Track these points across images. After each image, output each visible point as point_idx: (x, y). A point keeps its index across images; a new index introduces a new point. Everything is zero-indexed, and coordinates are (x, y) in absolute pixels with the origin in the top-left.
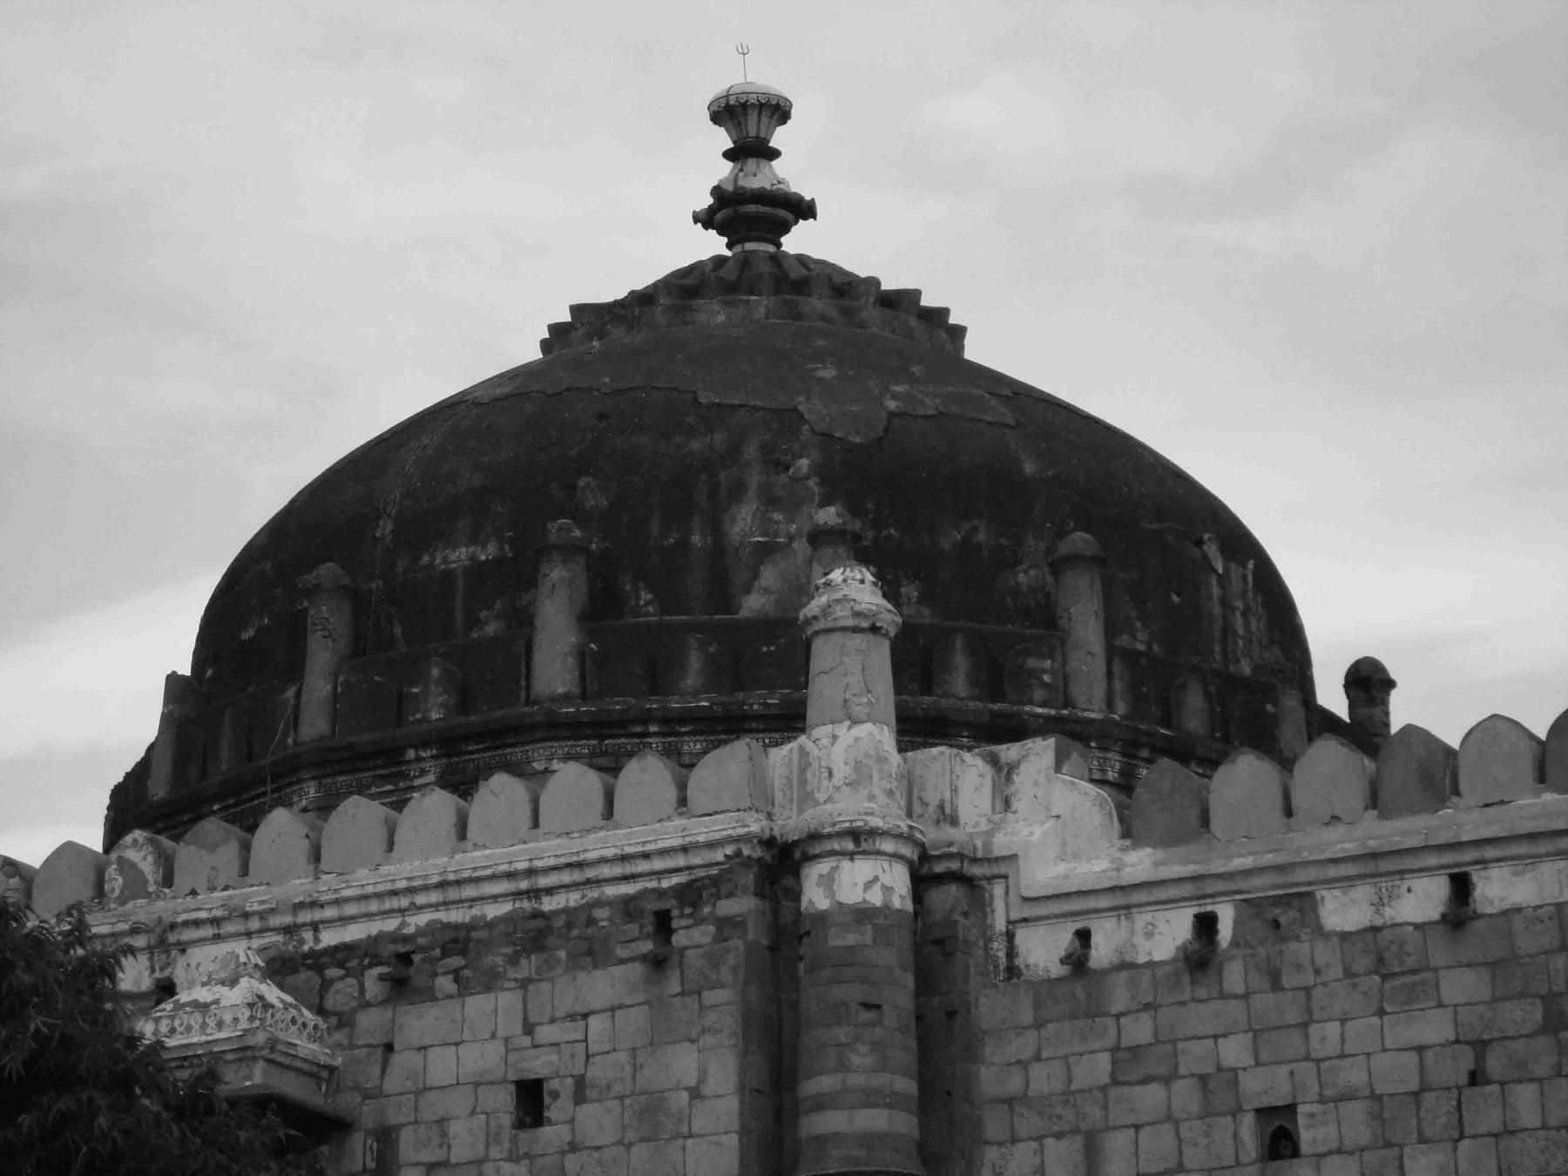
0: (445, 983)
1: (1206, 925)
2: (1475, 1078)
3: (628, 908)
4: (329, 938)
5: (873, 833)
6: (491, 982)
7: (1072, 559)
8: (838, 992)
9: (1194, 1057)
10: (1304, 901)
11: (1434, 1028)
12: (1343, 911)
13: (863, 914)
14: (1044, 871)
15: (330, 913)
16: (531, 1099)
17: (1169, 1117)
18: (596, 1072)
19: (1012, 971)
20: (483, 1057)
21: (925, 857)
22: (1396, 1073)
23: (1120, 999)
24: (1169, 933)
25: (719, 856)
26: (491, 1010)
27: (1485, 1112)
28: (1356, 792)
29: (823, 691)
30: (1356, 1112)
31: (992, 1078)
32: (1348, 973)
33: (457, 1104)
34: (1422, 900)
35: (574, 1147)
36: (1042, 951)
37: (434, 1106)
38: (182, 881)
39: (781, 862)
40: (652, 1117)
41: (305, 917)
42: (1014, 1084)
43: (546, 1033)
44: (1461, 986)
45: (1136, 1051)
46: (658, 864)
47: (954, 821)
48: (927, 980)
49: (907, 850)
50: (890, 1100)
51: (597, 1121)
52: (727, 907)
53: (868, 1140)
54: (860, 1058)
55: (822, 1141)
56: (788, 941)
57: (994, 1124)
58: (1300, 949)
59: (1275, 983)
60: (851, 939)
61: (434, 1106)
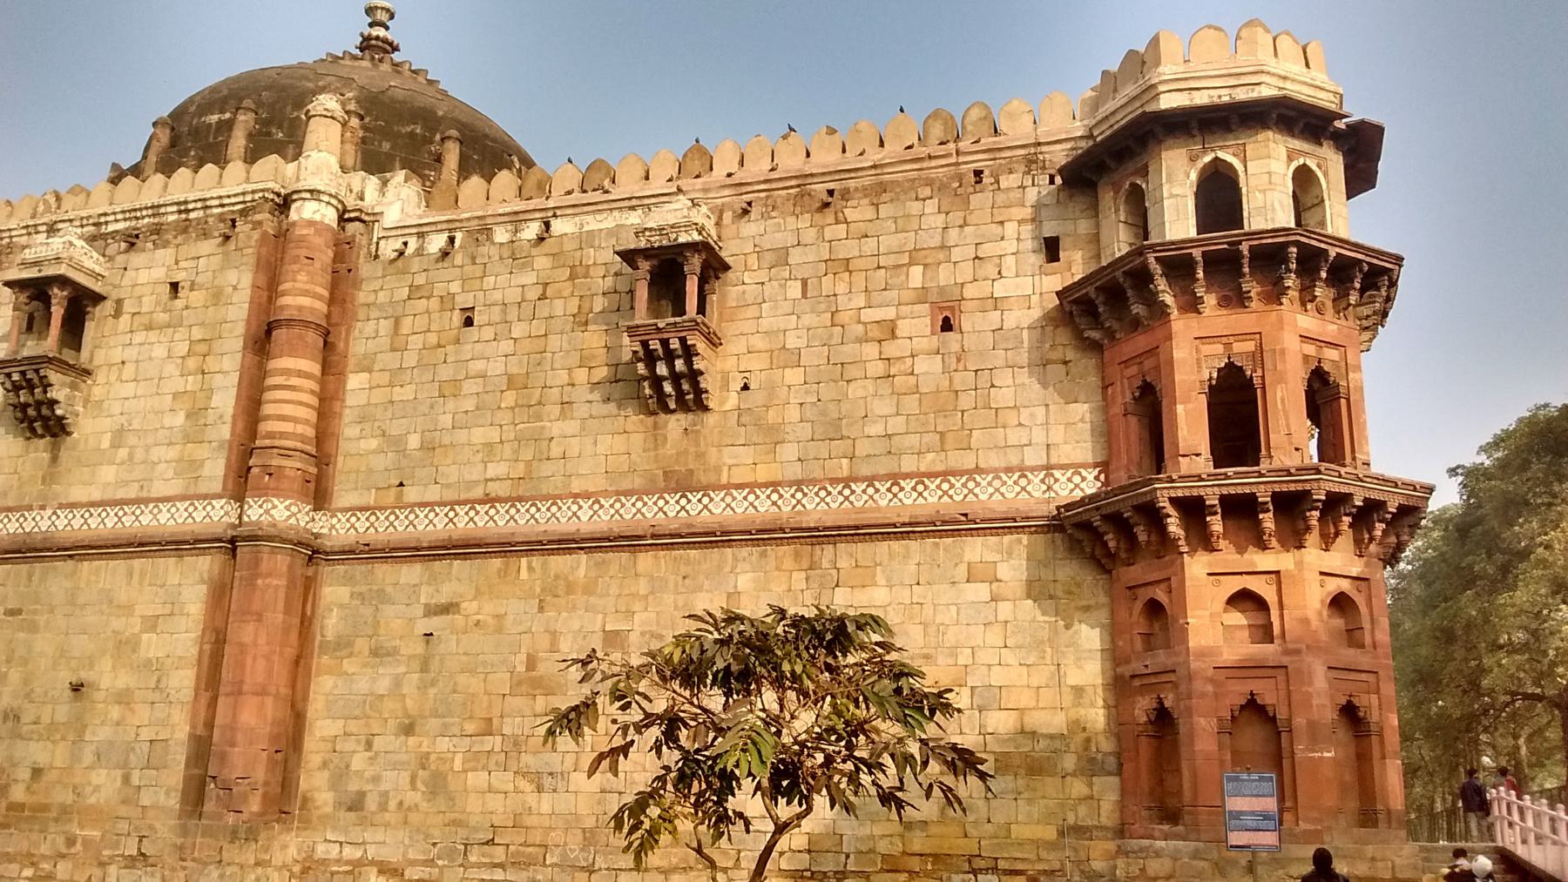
0: (150, 245)
1: (452, 240)
2: (543, 297)
3: (221, 218)
4: (111, 228)
5: (319, 192)
6: (166, 245)
7: (449, 138)
8: (297, 252)
9: (439, 289)
10: (487, 231)
11: (529, 278)
12: (501, 235)
13: (311, 223)
14: (392, 216)
15: (111, 218)
16: (175, 286)
17: (427, 312)
18: (199, 279)
19: (377, 257)
20: (159, 273)
21: (345, 211)
22: (513, 295)
23: (416, 265)
24: (437, 242)
25: (257, 196)
26: (166, 255)
27: (544, 309)
28: (514, 191)
29: (311, 139)
30: (497, 309)
31: (362, 296)
32: (501, 258)
33: (147, 290)
34: (532, 230)
35: (187, 308)
36: (388, 249)
37: (138, 291)
38: (63, 209)
39: (284, 204)
40: (217, 297)
41: (102, 220)
42: (371, 298)
43: (182, 264)
44: (542, 262)
45: (418, 287)
46: (233, 200)
47: (362, 199)
48: (339, 257)
49: (334, 202)
50: (320, 297)
51: (196, 298)
52: (258, 217)
53: (300, 308)
54: (302, 277)
55: (282, 308)
56: (282, 237)
57: (361, 314)
58: (484, 250)
59: (473, 258)
60: (305, 232)
61: (138, 291)
